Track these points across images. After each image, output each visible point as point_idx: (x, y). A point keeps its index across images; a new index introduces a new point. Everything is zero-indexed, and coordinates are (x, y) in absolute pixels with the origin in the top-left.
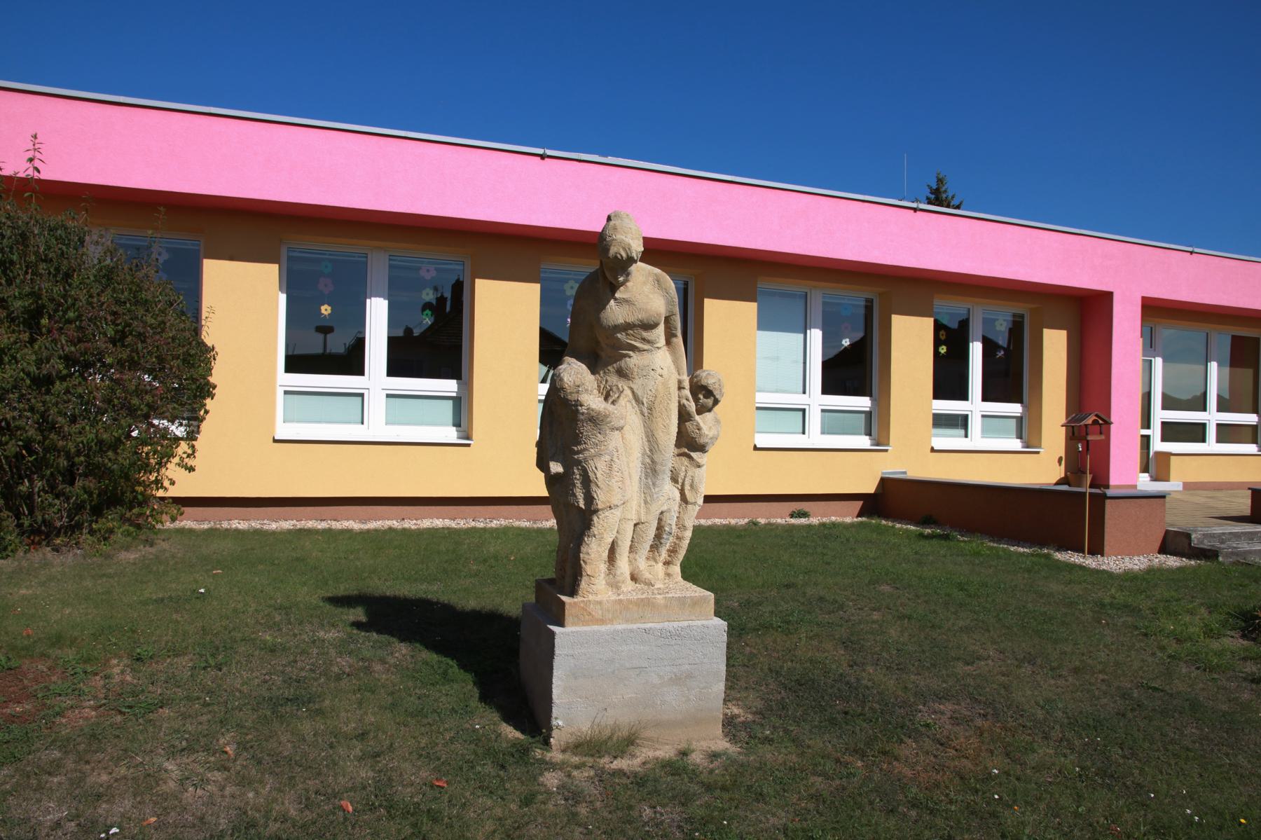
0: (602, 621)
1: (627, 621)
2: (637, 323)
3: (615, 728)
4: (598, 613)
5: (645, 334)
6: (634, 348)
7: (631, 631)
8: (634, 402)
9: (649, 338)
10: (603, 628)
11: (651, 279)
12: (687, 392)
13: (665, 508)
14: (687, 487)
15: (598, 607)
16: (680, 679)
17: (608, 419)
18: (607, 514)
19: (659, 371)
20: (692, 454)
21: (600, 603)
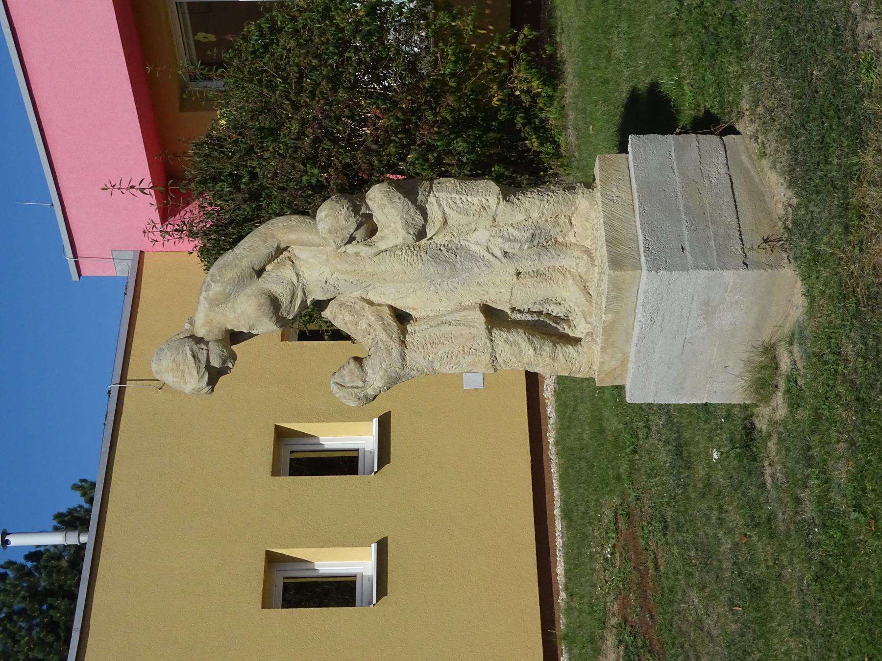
0: (624, 361)
1: (628, 341)
2: (274, 318)
3: (748, 362)
4: (614, 364)
5: (285, 301)
6: (304, 302)
7: (639, 351)
8: (369, 289)
9: (289, 298)
10: (631, 366)
11: (217, 310)
12: (350, 249)
13: (499, 254)
14: (473, 226)
15: (607, 364)
16: (708, 311)
17: (393, 375)
18: (500, 361)
19: (326, 275)
20: (429, 236)
21: (602, 363)
